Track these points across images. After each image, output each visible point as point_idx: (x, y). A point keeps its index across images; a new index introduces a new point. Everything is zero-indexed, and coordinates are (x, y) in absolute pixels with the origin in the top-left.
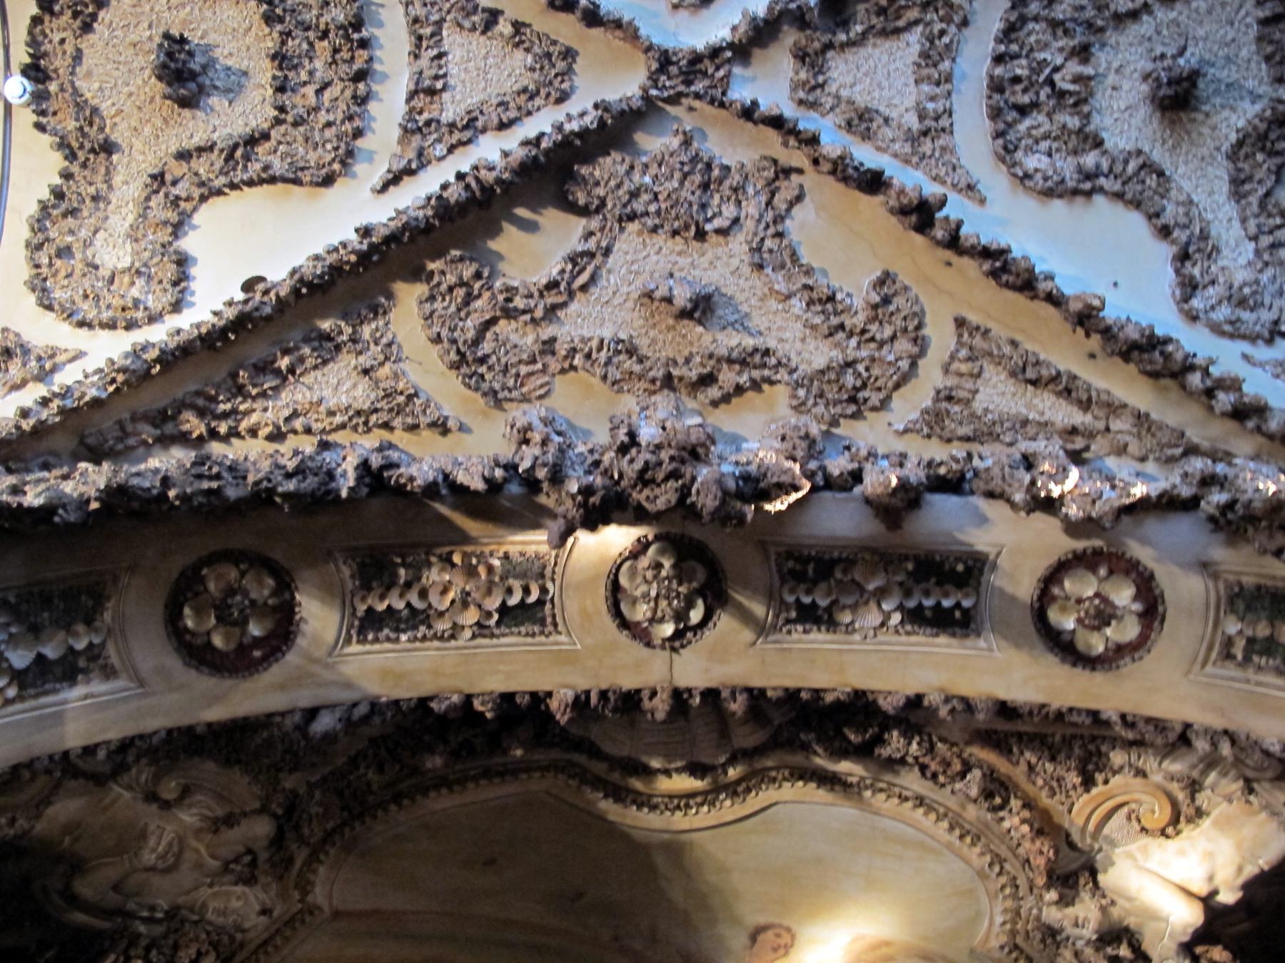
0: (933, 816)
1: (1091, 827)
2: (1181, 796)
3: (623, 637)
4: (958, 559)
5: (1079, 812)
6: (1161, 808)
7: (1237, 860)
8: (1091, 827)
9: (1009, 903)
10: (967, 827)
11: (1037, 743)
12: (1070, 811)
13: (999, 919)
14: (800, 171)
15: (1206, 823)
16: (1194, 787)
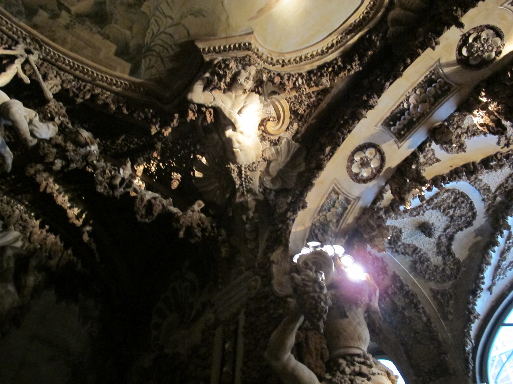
0: (315, 53)
1: (277, 103)
2: (272, 138)
3: (485, 23)
4: (405, 133)
5: (283, 102)
6: (273, 130)
7: (243, 144)
8: (277, 103)
9: (264, 57)
10: (304, 62)
11: (316, 103)
12: (286, 99)
13: (260, 49)
14: (502, 148)
15: (258, 140)
16: (275, 143)
